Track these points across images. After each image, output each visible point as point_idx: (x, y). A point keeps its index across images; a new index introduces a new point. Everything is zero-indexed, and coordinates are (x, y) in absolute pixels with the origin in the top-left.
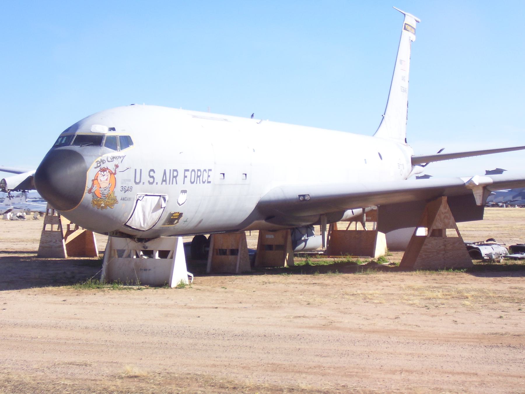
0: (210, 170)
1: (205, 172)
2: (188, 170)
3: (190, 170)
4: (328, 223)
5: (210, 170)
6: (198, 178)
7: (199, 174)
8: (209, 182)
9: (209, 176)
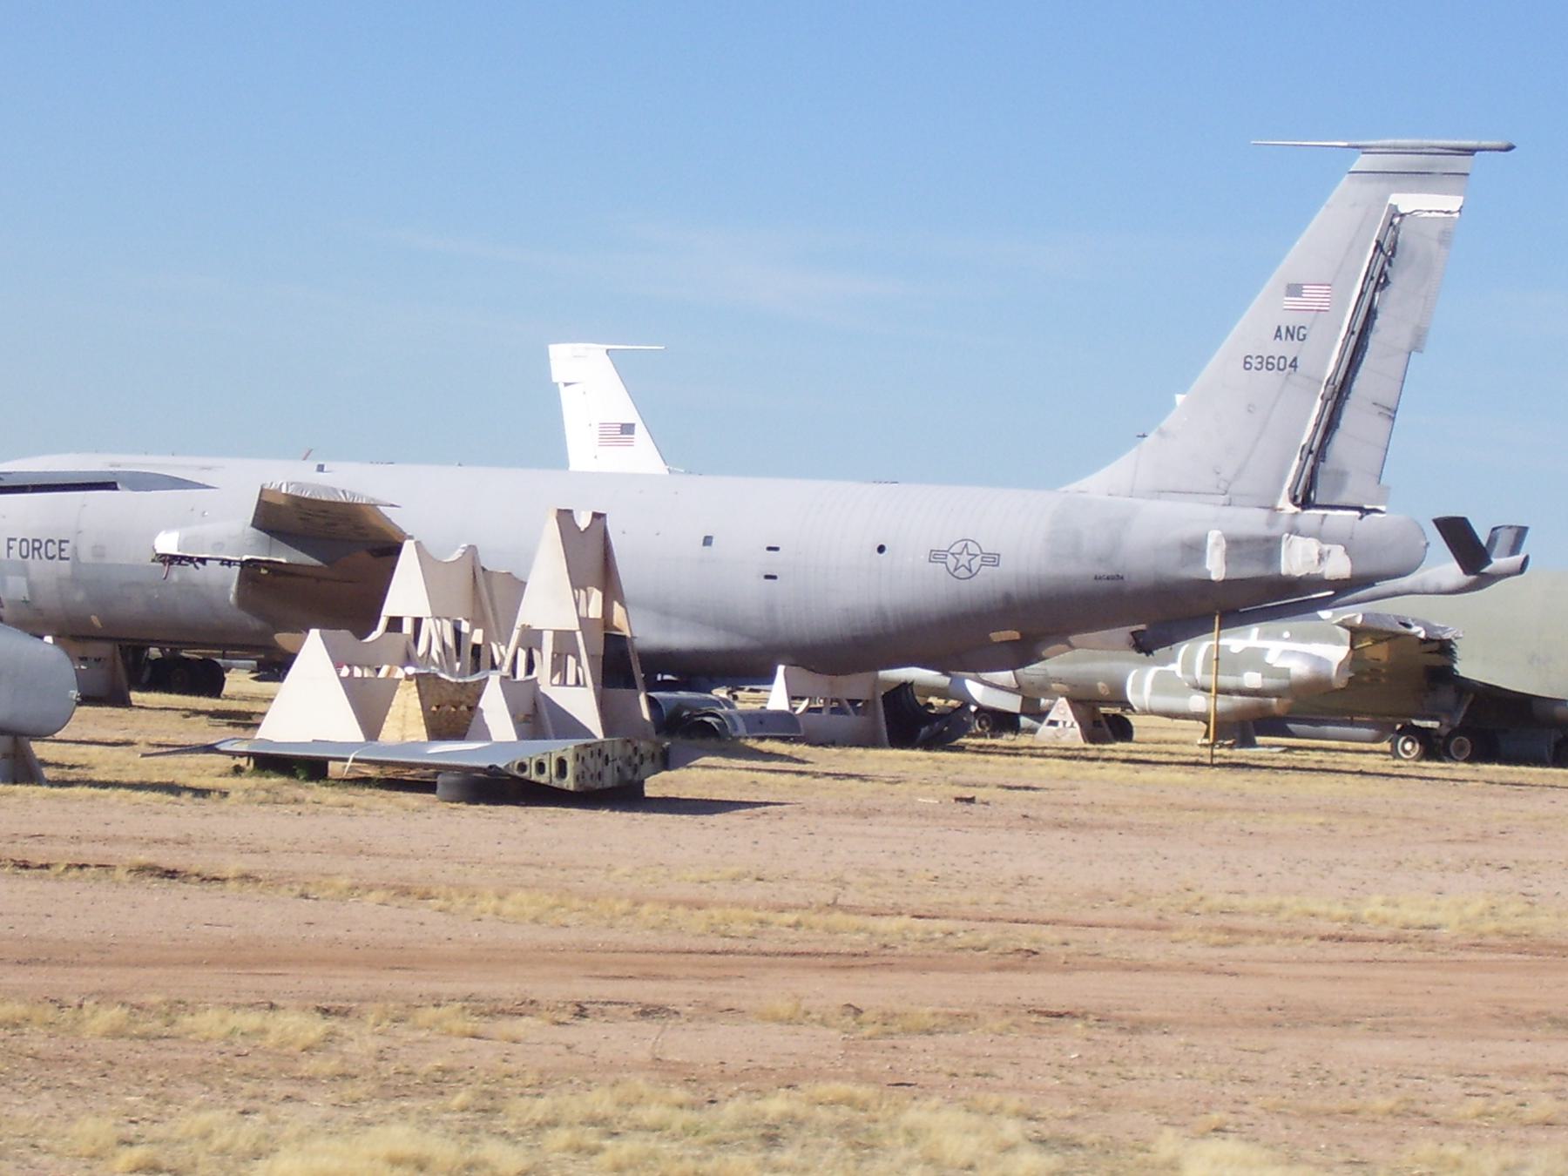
0: (67, 542)
1: (50, 544)
2: (15, 540)
3: (19, 540)
4: (1021, 634)
5: (67, 542)
6: (36, 553)
7: (37, 545)
8: (61, 558)
9: (61, 550)
